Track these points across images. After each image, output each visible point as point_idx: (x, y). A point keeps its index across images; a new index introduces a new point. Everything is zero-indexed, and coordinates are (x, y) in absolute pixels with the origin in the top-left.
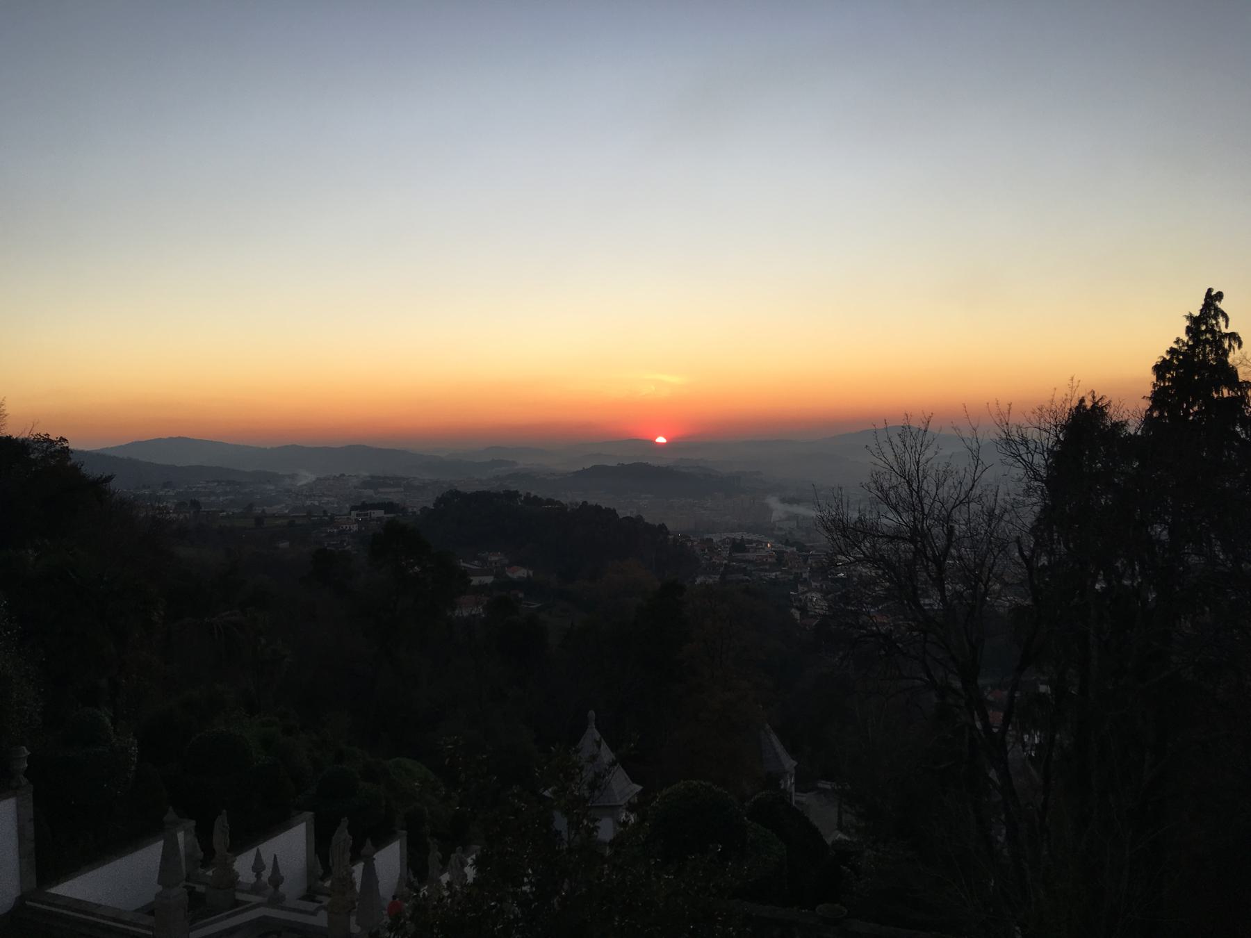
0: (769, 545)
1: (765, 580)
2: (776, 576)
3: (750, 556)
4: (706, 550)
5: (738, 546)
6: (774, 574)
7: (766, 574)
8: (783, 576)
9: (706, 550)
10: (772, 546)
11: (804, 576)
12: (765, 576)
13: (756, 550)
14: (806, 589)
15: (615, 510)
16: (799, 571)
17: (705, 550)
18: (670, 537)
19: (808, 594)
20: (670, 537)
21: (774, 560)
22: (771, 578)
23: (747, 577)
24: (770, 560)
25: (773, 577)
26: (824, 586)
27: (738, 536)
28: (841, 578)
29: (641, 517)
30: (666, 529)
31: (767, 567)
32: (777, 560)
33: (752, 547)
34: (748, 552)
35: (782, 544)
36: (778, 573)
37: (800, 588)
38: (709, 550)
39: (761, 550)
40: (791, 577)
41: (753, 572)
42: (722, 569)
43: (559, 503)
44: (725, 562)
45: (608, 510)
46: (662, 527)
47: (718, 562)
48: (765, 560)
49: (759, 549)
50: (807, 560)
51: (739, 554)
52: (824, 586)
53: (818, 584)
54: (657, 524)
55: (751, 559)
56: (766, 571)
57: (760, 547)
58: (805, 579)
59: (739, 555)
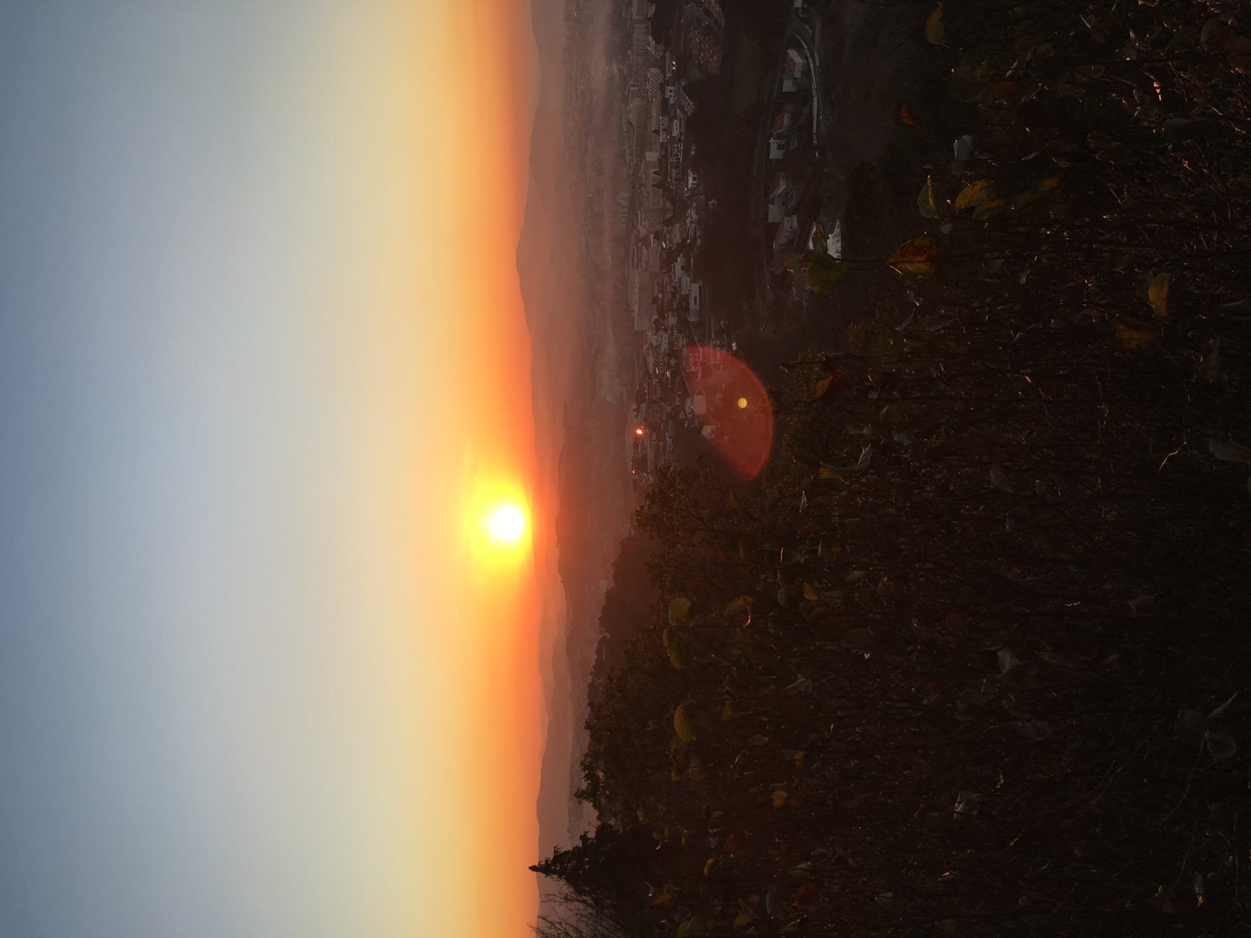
1: (674, 449)
2: (670, 438)
3: (650, 455)
5: (640, 464)
6: (667, 439)
8: (670, 432)
11: (669, 409)
13: (644, 448)
14: (682, 413)
16: (665, 414)
19: (687, 413)
24: (654, 437)
26: (679, 393)
28: (672, 374)
31: (661, 444)
34: (646, 455)
36: (667, 435)
37: (682, 416)
40: (671, 422)
41: (667, 458)
50: (653, 401)
52: (679, 393)
53: (677, 399)
56: (665, 445)
58: (673, 409)
59: (650, 465)
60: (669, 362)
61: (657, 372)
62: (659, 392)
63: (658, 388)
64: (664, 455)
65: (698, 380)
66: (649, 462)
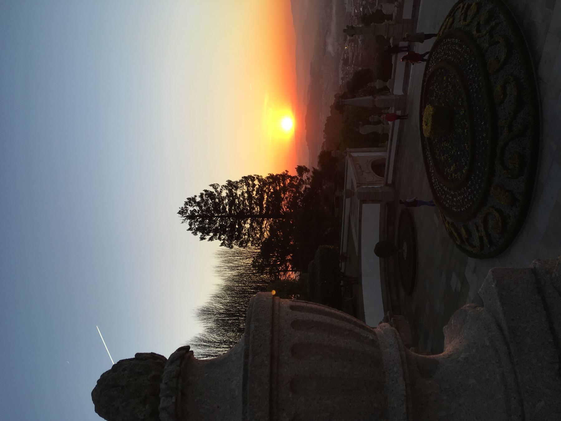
0: (346, 48)
2: (360, 41)
3: (350, 55)
4: (347, 76)
6: (359, 41)
7: (359, 46)
9: (347, 76)
10: (347, 47)
12: (360, 46)
15: (328, 117)
17: (347, 77)
18: (340, 93)
20: (340, 93)
21: (353, 44)
22: (361, 43)
23: (361, 54)
24: (353, 45)
25: (361, 42)
27: (341, 62)
28: (363, 9)
29: (331, 106)
30: (337, 94)
31: (356, 45)
32: (353, 42)
33: (346, 55)
35: (346, 42)
36: (359, 40)
38: (347, 75)
39: (348, 50)
42: (356, 67)
43: (323, 144)
44: (353, 66)
45: (327, 120)
46: (335, 96)
47: (353, 69)
48: (353, 48)
49: (347, 52)
51: (350, 60)
54: (335, 99)
55: (352, 55)
56: (357, 46)
57: (346, 52)
60: (362, 3)
61: (356, 12)
62: (356, 22)
63: (356, 20)
64: (357, 50)
65: (375, 7)
66: (350, 58)
